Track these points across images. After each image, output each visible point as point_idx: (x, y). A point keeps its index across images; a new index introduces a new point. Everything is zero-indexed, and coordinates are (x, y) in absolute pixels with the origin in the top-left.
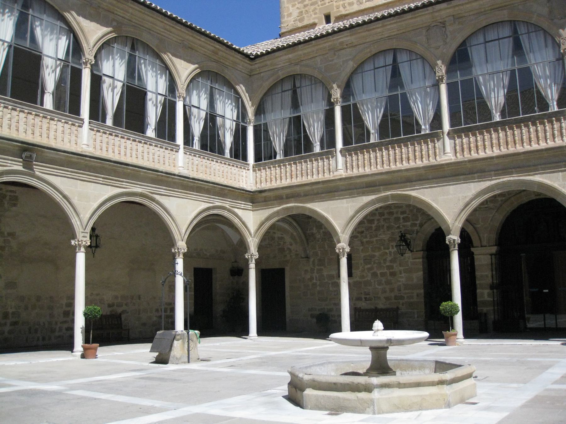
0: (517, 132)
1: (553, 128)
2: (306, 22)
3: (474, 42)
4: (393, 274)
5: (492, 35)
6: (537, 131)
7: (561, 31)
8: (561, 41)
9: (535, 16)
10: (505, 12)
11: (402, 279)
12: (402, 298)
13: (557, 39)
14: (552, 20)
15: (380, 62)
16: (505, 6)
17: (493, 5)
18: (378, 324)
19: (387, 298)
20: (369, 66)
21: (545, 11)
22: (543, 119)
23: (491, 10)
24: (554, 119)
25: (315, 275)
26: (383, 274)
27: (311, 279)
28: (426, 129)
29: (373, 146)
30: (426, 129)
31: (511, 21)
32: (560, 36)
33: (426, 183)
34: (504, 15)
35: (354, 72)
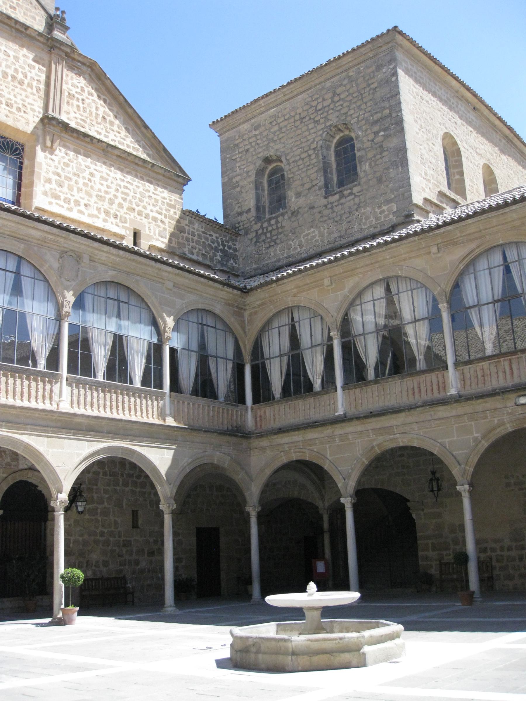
0: (11, 381)
1: (44, 389)
6: (29, 387)
7: (66, 291)
8: (65, 303)
9: (47, 266)
10: (22, 246)
13: (60, 299)
14: (61, 277)
16: (23, 239)
17: (13, 232)
18: (312, 586)
21: (56, 265)
22: (38, 376)
23: (8, 235)
24: (47, 379)
31: (20, 257)
32: (64, 297)
33: (80, 434)
34: (19, 249)
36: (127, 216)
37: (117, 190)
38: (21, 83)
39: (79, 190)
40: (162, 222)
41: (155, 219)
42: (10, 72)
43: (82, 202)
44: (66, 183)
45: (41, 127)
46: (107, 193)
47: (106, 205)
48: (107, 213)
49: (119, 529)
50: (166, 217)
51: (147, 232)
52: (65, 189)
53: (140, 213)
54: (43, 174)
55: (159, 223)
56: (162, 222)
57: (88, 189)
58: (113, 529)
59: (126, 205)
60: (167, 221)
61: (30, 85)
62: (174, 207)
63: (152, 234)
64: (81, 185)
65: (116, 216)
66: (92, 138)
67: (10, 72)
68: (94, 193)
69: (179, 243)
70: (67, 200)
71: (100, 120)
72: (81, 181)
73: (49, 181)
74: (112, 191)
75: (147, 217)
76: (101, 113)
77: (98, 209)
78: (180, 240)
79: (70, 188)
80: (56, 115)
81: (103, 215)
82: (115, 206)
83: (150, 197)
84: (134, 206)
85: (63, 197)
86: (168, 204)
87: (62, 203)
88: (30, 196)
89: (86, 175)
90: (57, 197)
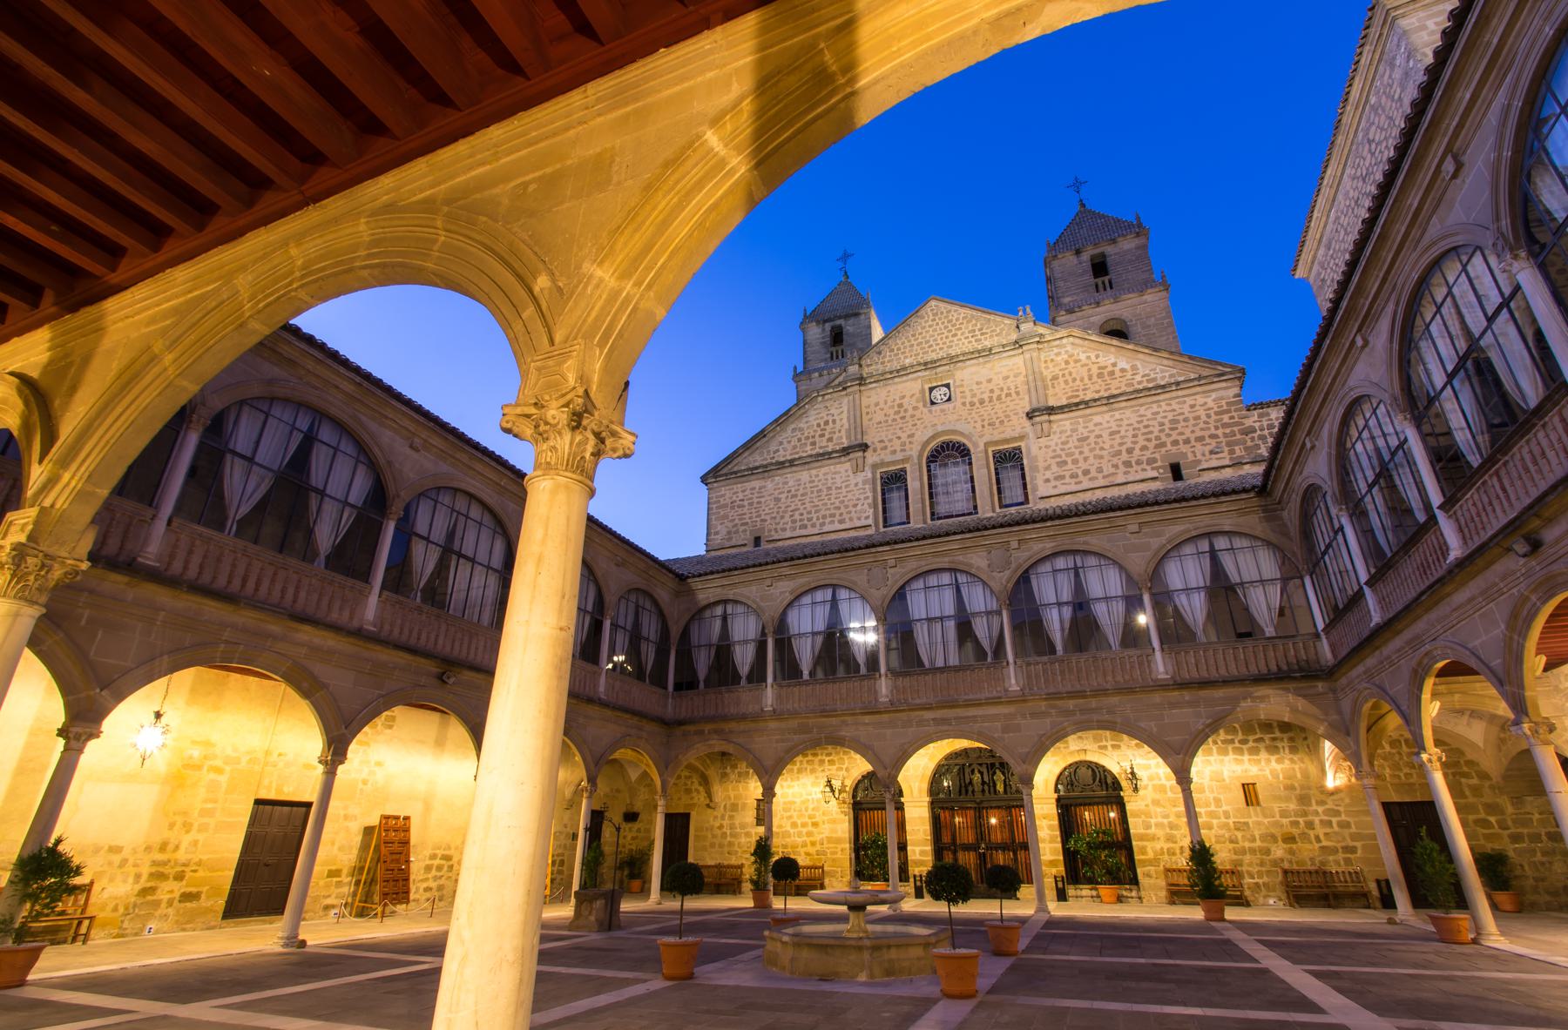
2: (733, 543)
3: (915, 585)
4: (815, 824)
5: (933, 580)
11: (825, 831)
12: (824, 853)
15: (819, 596)
19: (807, 854)
20: (807, 600)
25: (726, 822)
26: (804, 825)
27: (721, 827)
28: (863, 670)
29: (807, 683)
30: (863, 670)
34: (944, 562)
35: (790, 605)
36: (1157, 456)
37: (1135, 436)
38: (999, 398)
39: (1086, 459)
40: (1212, 436)
41: (1200, 439)
42: (986, 396)
43: (1093, 470)
44: (1069, 460)
45: (1027, 423)
46: (1121, 444)
47: (1125, 456)
48: (1127, 464)
49: (1225, 808)
50: (1217, 428)
51: (1191, 457)
52: (1070, 466)
53: (1175, 443)
54: (1041, 464)
55: (1208, 440)
56: (1212, 436)
57: (1098, 452)
58: (1213, 808)
59: (1151, 445)
60: (1220, 432)
61: (1008, 395)
62: (1228, 411)
63: (1199, 457)
64: (1087, 453)
65: (1138, 463)
66: (1086, 403)
67: (986, 396)
68: (1104, 453)
69: (1246, 449)
70: (1072, 476)
71: (1095, 378)
72: (1086, 450)
73: (1048, 468)
74: (1129, 440)
75: (1187, 441)
76: (1095, 371)
77: (1116, 466)
78: (1249, 443)
79: (1075, 462)
80: (1042, 404)
81: (1122, 469)
82: (1137, 452)
83: (1186, 420)
84: (1164, 439)
85: (1067, 474)
86: (1217, 413)
87: (1067, 480)
88: (1035, 489)
89: (1092, 440)
90: (1063, 477)
